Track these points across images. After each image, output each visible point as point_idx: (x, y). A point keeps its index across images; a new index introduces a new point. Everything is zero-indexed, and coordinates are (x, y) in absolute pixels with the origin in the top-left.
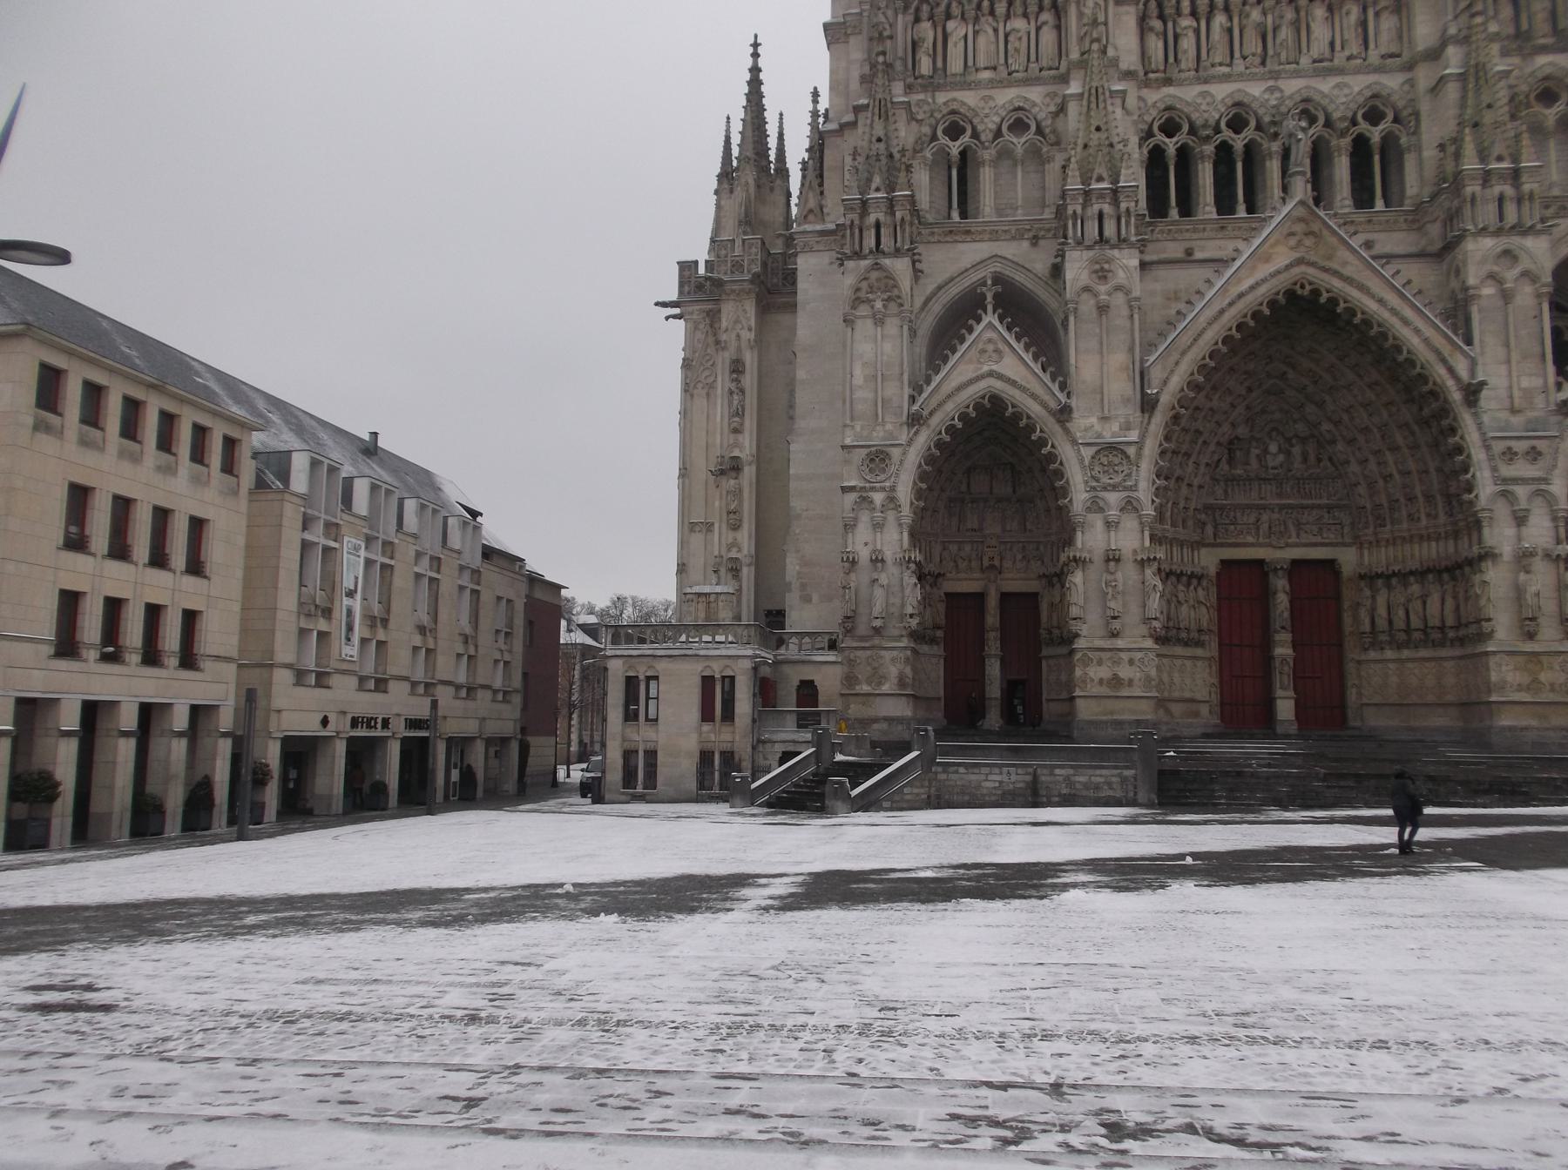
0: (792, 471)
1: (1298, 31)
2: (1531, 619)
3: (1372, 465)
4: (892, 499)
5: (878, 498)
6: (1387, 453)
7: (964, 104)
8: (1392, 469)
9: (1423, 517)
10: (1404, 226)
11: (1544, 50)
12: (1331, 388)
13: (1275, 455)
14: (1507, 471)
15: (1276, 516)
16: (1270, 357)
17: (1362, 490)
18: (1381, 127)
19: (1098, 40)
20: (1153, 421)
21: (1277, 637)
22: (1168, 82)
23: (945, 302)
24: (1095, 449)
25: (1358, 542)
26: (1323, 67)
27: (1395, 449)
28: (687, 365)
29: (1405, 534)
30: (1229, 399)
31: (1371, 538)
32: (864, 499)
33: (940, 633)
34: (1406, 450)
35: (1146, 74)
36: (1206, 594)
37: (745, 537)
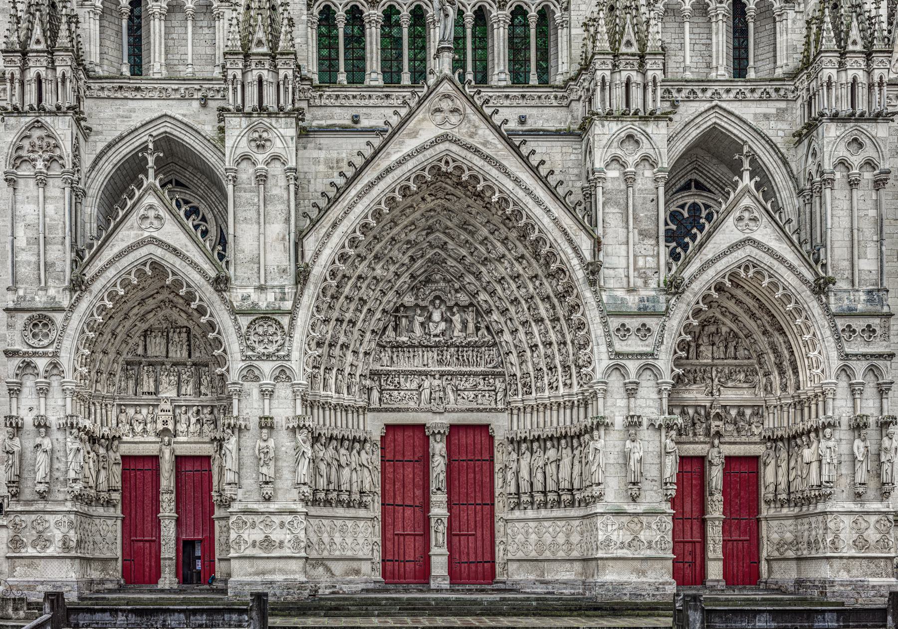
2: (634, 484)
3: (521, 335)
6: (533, 324)
8: (538, 339)
9: (561, 385)
12: (486, 259)
13: (438, 323)
15: (436, 382)
17: (513, 358)
20: (306, 292)
23: (115, 161)
24: (251, 318)
25: (509, 409)
27: (539, 321)
29: (547, 402)
30: (393, 268)
31: (520, 405)
34: (547, 322)
36: (372, 457)
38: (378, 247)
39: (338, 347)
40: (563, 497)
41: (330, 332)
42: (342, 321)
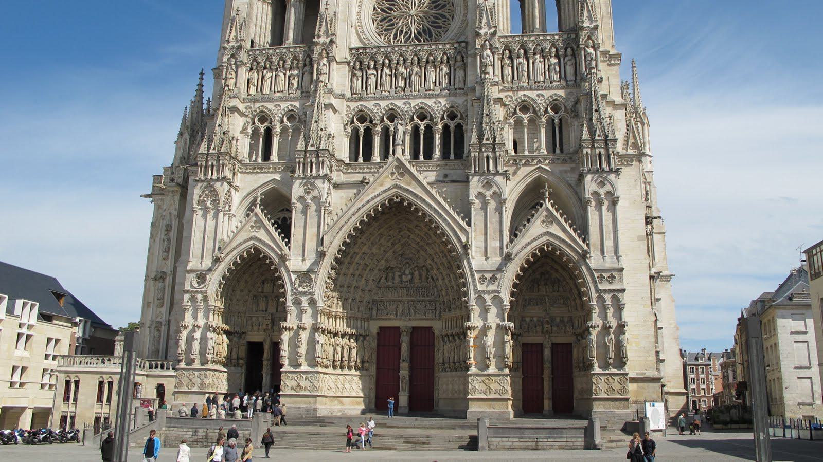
0: (177, 281)
1: (421, 77)
4: (206, 297)
5: (199, 297)
7: (267, 108)
10: (462, 167)
11: (521, 88)
14: (480, 287)
16: (401, 228)
17: (444, 293)
18: (455, 121)
19: (322, 82)
21: (402, 365)
22: (361, 99)
26: (429, 94)
28: (153, 225)
32: (194, 296)
33: (241, 362)
35: (352, 95)
37: (164, 310)
38: (372, 239)
39: (352, 288)
40: (462, 365)
41: (347, 281)
42: (354, 275)
